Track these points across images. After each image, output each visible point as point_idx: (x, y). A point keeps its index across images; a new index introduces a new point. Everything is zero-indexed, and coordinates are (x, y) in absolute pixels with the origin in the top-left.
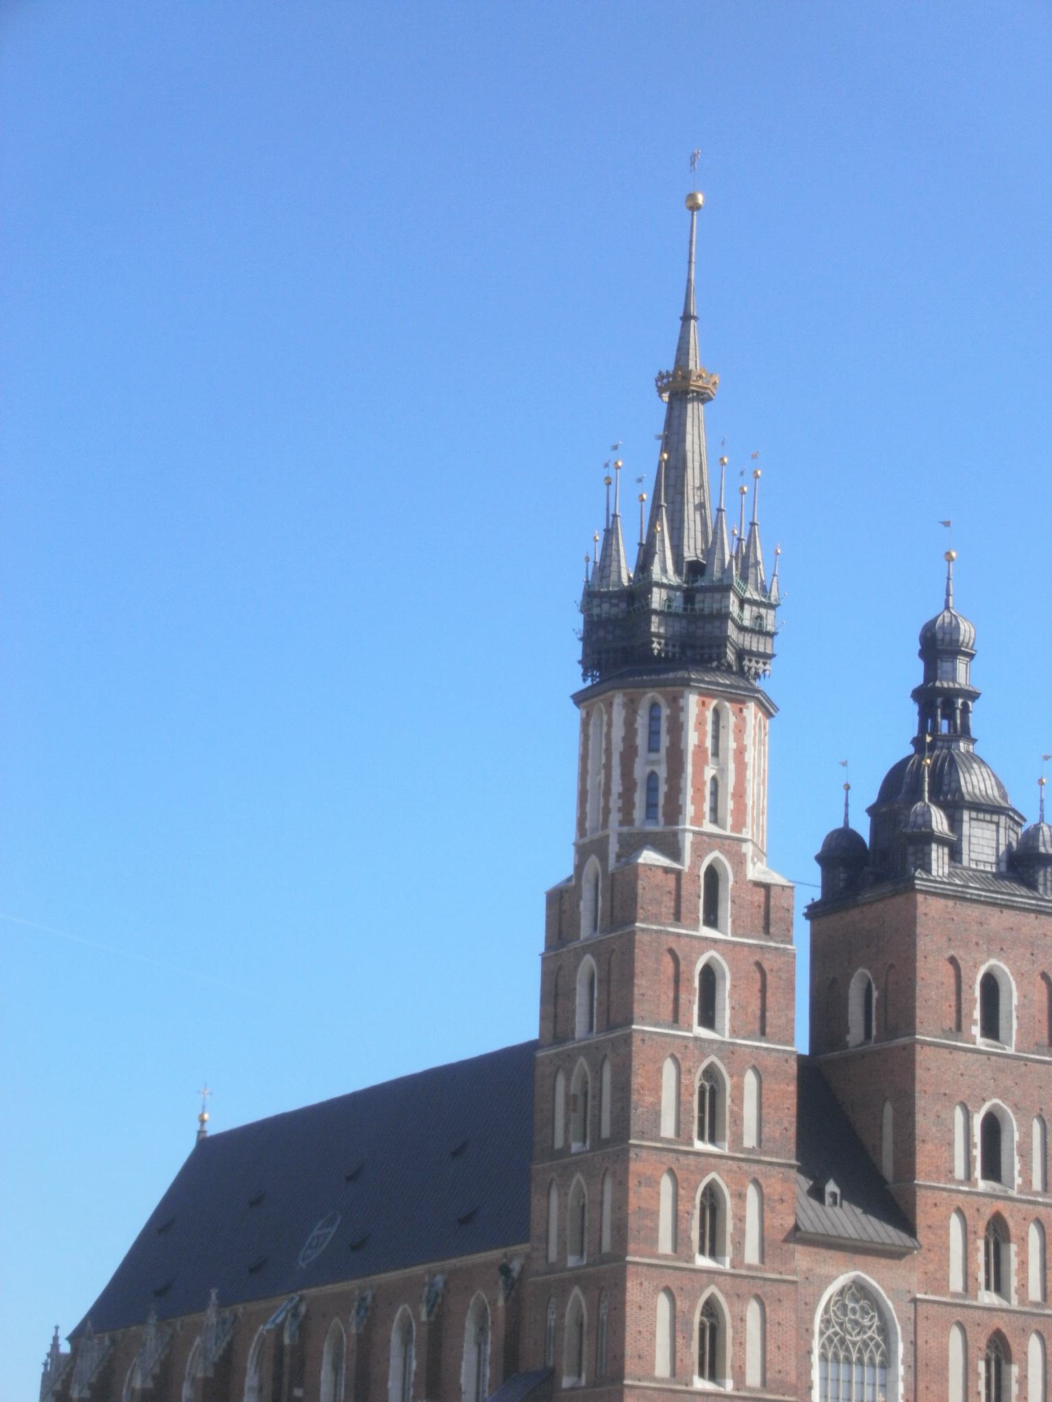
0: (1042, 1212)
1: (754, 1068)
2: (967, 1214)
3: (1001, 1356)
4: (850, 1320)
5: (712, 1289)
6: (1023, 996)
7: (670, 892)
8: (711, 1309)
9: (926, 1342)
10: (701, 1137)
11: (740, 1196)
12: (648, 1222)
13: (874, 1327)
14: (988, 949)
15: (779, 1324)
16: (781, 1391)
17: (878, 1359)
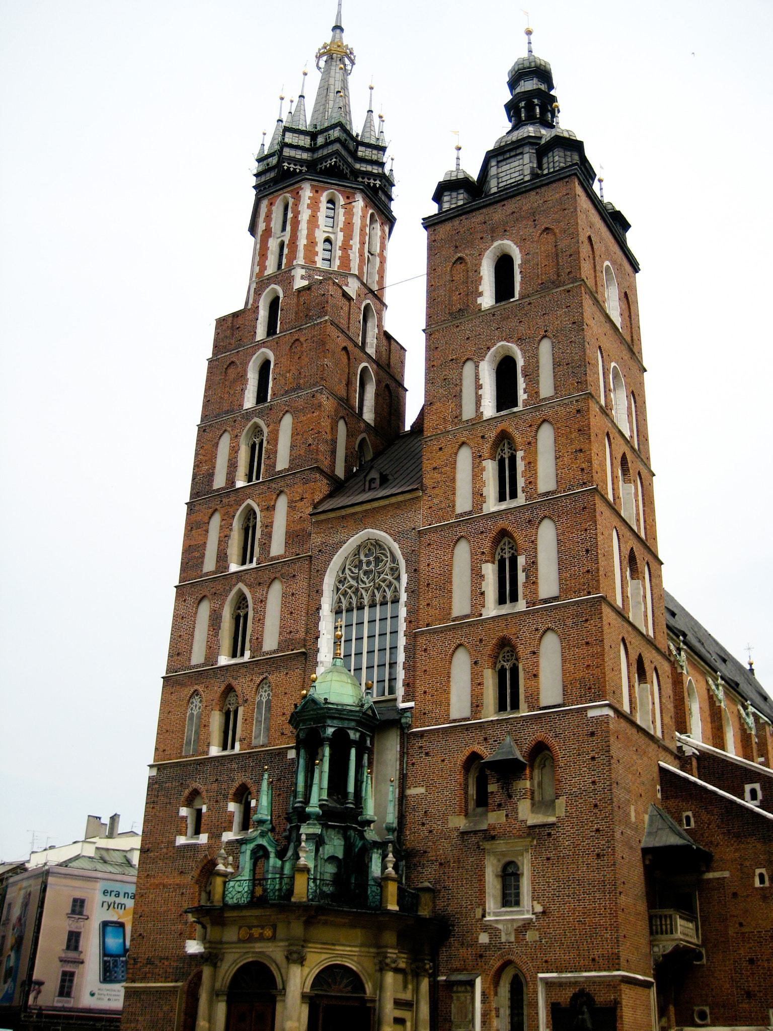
0: (548, 412)
1: (287, 411)
2: (472, 444)
3: (516, 554)
4: (366, 573)
5: (241, 585)
6: (525, 253)
7: (239, 328)
8: (241, 601)
9: (428, 565)
10: (250, 480)
11: (270, 509)
12: (196, 554)
13: (387, 570)
14: (492, 237)
15: (293, 594)
16: (290, 647)
17: (389, 594)
